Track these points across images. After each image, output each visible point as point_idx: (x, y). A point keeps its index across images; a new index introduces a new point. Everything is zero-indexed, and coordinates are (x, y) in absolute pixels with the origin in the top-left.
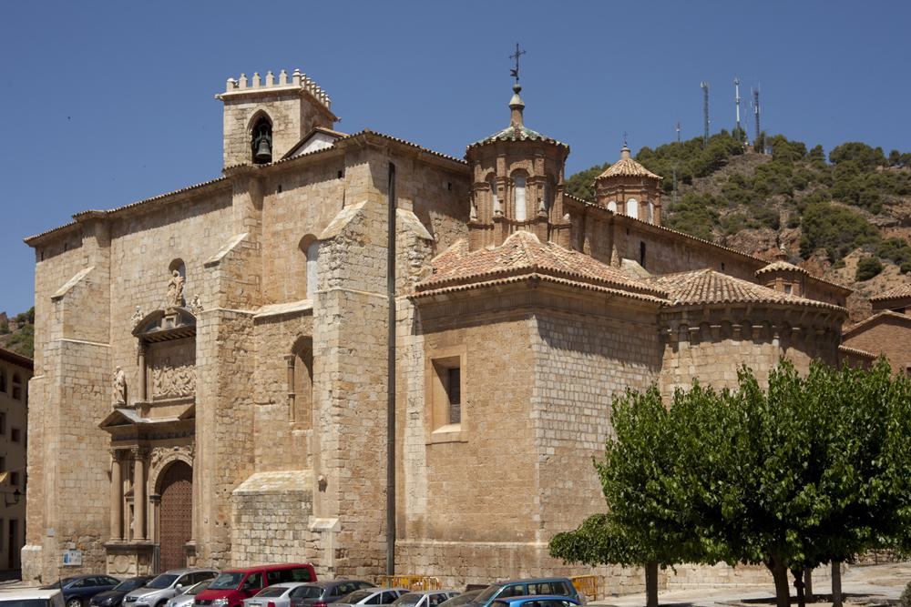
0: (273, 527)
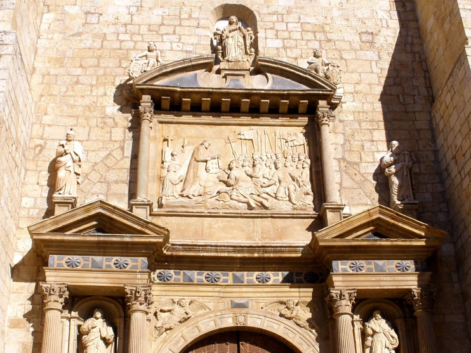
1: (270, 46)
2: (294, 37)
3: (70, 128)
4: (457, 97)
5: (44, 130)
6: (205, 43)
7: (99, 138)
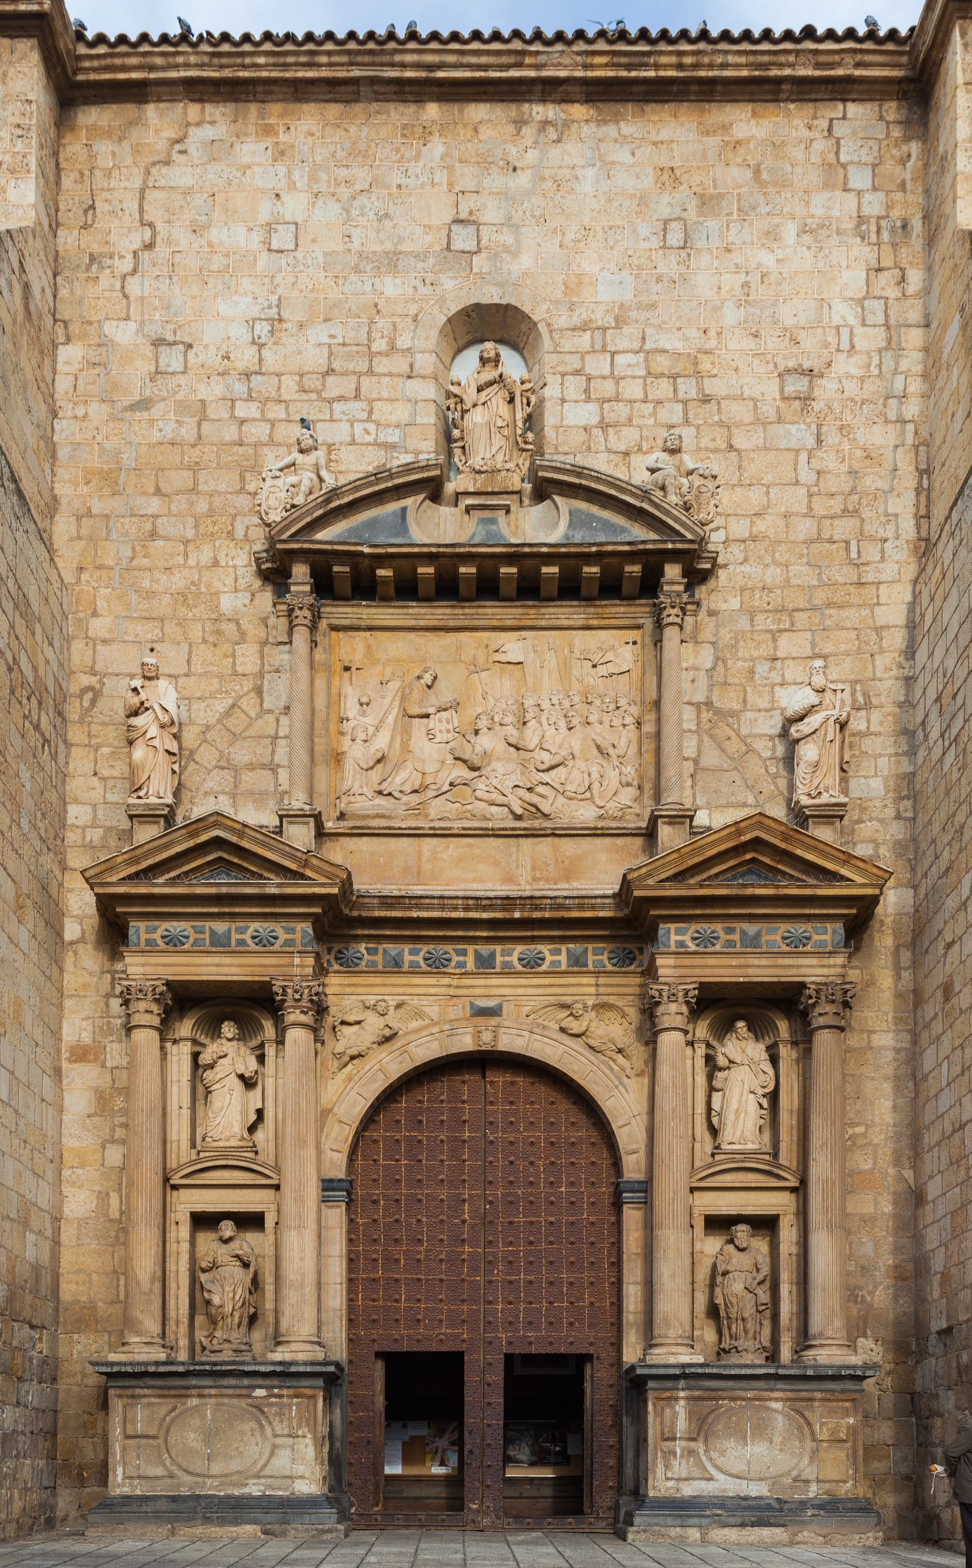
1: (571, 424)
2: (626, 396)
3: (149, 646)
5: (94, 650)
6: (425, 421)
7: (210, 668)
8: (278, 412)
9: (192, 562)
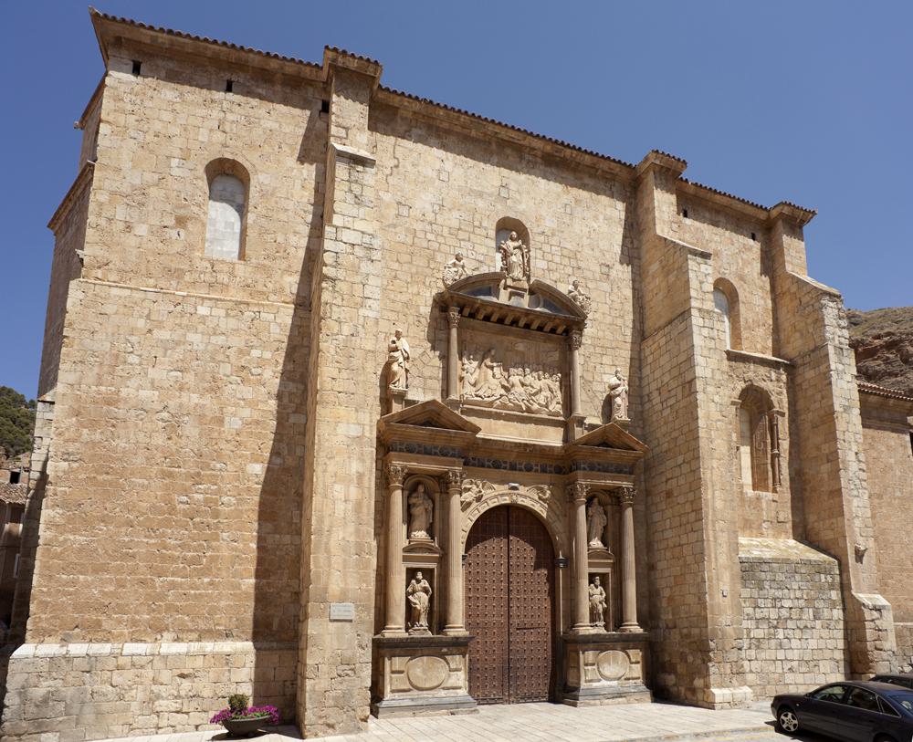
0: (787, 604)
4: (672, 343)
8: (441, 240)
9: (410, 291)
